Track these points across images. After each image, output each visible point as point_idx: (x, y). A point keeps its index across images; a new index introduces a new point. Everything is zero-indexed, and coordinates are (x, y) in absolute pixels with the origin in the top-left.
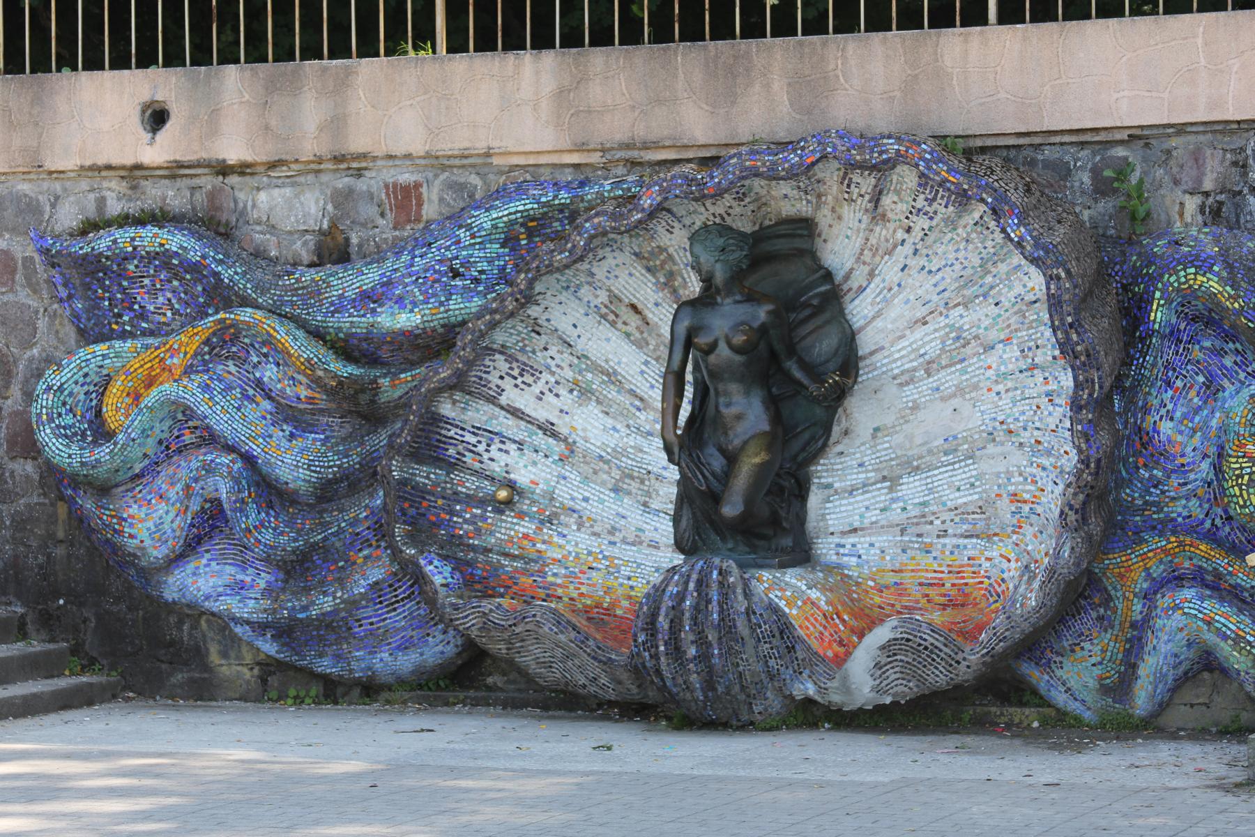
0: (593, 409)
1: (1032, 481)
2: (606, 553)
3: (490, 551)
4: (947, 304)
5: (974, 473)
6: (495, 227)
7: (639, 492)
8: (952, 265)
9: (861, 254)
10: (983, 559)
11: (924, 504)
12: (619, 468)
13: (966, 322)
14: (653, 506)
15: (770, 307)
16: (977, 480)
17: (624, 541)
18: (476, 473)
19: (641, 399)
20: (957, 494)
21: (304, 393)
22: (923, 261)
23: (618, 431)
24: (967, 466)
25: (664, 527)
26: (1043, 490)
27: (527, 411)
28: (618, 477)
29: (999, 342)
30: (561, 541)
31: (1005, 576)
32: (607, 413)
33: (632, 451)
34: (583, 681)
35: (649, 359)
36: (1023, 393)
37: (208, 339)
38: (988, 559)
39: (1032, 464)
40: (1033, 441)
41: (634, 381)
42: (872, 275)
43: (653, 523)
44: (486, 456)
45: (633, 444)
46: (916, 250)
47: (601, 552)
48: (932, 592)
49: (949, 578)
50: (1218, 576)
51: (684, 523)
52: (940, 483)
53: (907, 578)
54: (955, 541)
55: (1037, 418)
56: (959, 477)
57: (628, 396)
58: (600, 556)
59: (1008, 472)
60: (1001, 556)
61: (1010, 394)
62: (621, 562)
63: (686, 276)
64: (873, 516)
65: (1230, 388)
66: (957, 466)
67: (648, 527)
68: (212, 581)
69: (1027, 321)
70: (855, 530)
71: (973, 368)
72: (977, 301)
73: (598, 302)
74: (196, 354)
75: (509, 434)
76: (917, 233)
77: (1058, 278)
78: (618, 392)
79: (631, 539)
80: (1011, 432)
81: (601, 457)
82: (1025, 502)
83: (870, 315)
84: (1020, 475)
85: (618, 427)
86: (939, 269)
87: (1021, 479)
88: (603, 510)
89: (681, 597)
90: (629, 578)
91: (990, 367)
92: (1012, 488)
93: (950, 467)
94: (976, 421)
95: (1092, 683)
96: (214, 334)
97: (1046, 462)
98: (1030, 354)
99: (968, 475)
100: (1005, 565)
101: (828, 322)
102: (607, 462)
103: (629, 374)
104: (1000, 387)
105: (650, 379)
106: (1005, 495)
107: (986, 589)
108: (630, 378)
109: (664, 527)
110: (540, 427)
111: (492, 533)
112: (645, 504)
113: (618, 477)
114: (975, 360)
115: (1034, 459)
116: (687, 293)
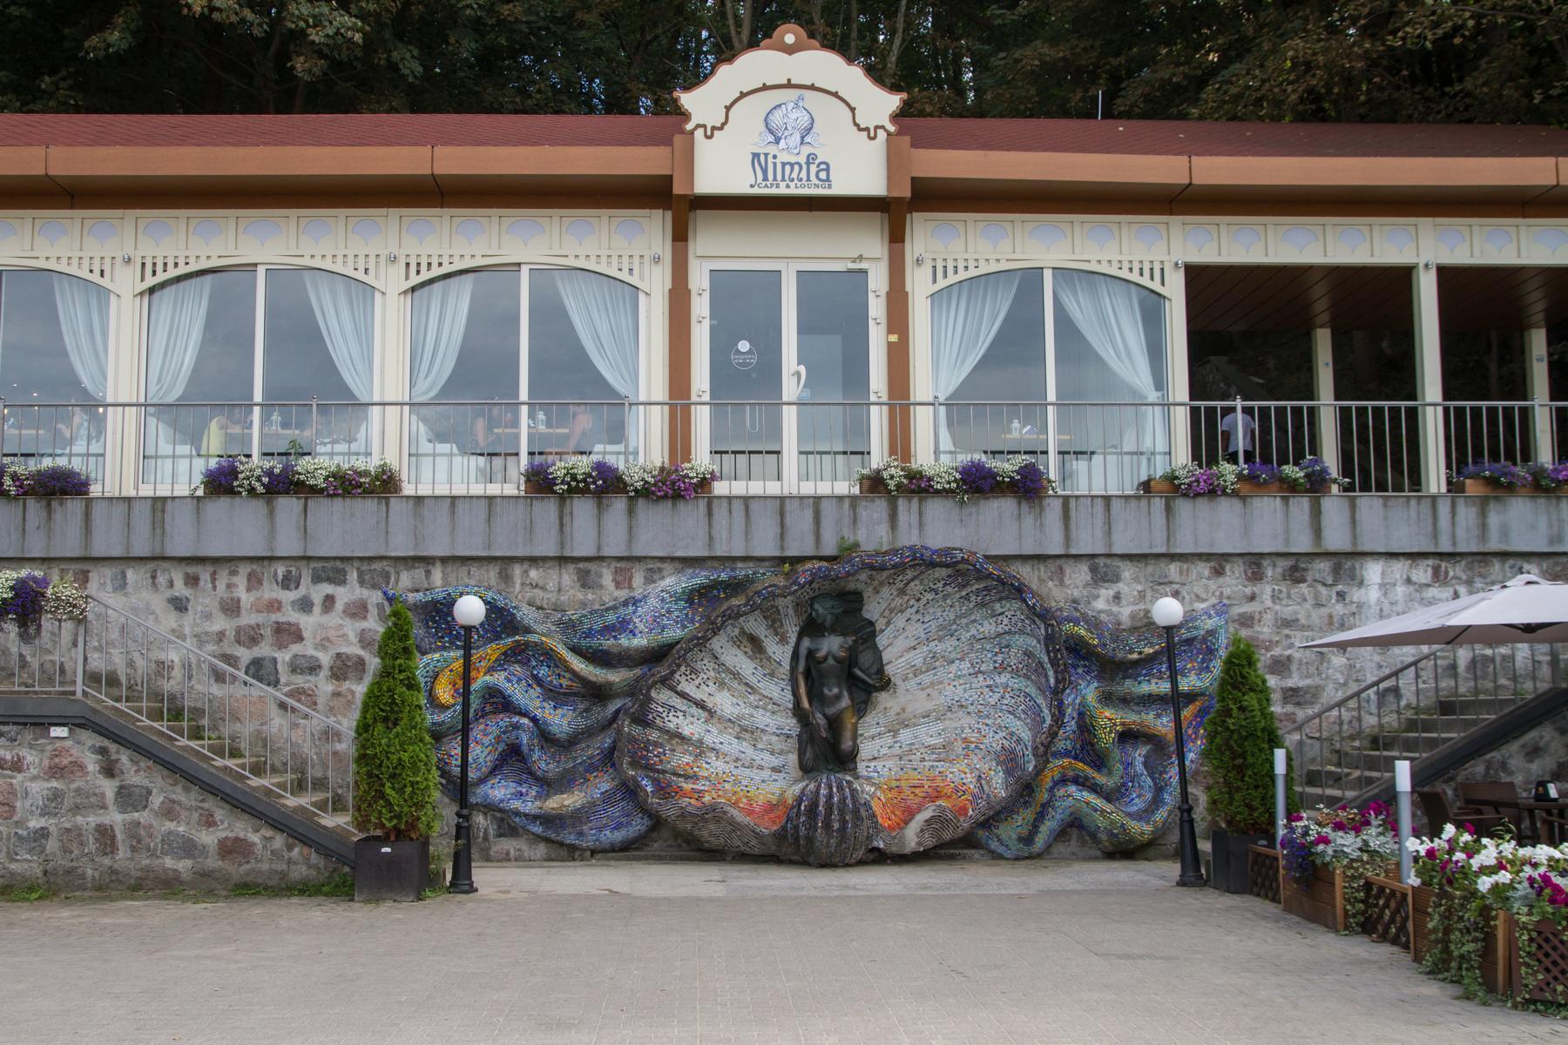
0: (725, 693)
3: (666, 772)
6: (684, 592)
11: (912, 744)
12: (739, 725)
13: (938, 650)
15: (854, 638)
17: (743, 766)
18: (660, 729)
19: (752, 688)
21: (565, 682)
22: (919, 616)
27: (691, 694)
30: (708, 766)
31: (965, 781)
34: (739, 843)
37: (506, 652)
38: (951, 773)
42: (888, 624)
44: (666, 719)
48: (917, 791)
50: (1086, 778)
51: (808, 755)
53: (903, 784)
54: (931, 763)
59: (962, 727)
61: (963, 686)
64: (884, 751)
65: (1084, 684)
68: (503, 792)
70: (875, 758)
73: (733, 635)
74: (496, 660)
75: (678, 707)
76: (924, 601)
77: (1053, 625)
80: (962, 706)
82: (972, 742)
83: (886, 644)
89: (830, 796)
92: (964, 736)
94: (942, 700)
95: (1014, 836)
96: (510, 649)
97: (989, 722)
100: (963, 776)
101: (867, 648)
102: (733, 723)
104: (956, 683)
110: (695, 703)
111: (669, 762)
112: (754, 745)
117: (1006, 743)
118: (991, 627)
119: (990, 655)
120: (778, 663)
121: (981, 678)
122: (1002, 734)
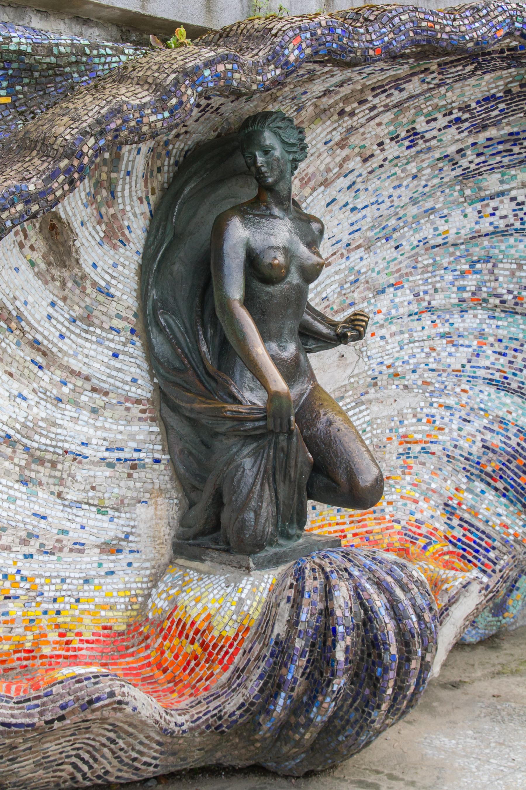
1: (428, 421)
2: (24, 573)
4: (348, 245)
5: (367, 418)
7: (51, 481)
8: (383, 202)
12: (27, 449)
13: (362, 266)
14: (69, 497)
16: (368, 425)
23: (24, 399)
24: (361, 412)
25: (91, 523)
26: (440, 429)
28: (23, 463)
29: (389, 286)
31: (418, 516)
32: (11, 375)
33: (43, 425)
35: (55, 299)
36: (411, 336)
39: (431, 405)
40: (420, 382)
41: (40, 329)
43: (78, 519)
45: (43, 415)
46: (354, 183)
47: (19, 571)
49: (352, 528)
55: (431, 360)
57: (28, 349)
58: (18, 578)
60: (402, 497)
61: (398, 338)
62: (43, 580)
63: (119, 188)
67: (73, 526)
69: (419, 265)
72: (379, 244)
78: (18, 344)
79: (47, 548)
80: (396, 375)
81: (9, 436)
82: (416, 442)
85: (25, 393)
88: (17, 513)
90: (55, 600)
91: (379, 312)
92: (402, 431)
97: (451, 401)
98: (427, 298)
99: (362, 421)
103: (35, 319)
104: (383, 332)
105: (59, 326)
107: (399, 533)
108: (36, 325)
109: (91, 523)
112: (59, 495)
113: (23, 463)
115: (434, 400)
116: (112, 211)
117: (495, 440)
118: (465, 221)
119: (449, 277)
120: (100, 290)
122: (478, 423)
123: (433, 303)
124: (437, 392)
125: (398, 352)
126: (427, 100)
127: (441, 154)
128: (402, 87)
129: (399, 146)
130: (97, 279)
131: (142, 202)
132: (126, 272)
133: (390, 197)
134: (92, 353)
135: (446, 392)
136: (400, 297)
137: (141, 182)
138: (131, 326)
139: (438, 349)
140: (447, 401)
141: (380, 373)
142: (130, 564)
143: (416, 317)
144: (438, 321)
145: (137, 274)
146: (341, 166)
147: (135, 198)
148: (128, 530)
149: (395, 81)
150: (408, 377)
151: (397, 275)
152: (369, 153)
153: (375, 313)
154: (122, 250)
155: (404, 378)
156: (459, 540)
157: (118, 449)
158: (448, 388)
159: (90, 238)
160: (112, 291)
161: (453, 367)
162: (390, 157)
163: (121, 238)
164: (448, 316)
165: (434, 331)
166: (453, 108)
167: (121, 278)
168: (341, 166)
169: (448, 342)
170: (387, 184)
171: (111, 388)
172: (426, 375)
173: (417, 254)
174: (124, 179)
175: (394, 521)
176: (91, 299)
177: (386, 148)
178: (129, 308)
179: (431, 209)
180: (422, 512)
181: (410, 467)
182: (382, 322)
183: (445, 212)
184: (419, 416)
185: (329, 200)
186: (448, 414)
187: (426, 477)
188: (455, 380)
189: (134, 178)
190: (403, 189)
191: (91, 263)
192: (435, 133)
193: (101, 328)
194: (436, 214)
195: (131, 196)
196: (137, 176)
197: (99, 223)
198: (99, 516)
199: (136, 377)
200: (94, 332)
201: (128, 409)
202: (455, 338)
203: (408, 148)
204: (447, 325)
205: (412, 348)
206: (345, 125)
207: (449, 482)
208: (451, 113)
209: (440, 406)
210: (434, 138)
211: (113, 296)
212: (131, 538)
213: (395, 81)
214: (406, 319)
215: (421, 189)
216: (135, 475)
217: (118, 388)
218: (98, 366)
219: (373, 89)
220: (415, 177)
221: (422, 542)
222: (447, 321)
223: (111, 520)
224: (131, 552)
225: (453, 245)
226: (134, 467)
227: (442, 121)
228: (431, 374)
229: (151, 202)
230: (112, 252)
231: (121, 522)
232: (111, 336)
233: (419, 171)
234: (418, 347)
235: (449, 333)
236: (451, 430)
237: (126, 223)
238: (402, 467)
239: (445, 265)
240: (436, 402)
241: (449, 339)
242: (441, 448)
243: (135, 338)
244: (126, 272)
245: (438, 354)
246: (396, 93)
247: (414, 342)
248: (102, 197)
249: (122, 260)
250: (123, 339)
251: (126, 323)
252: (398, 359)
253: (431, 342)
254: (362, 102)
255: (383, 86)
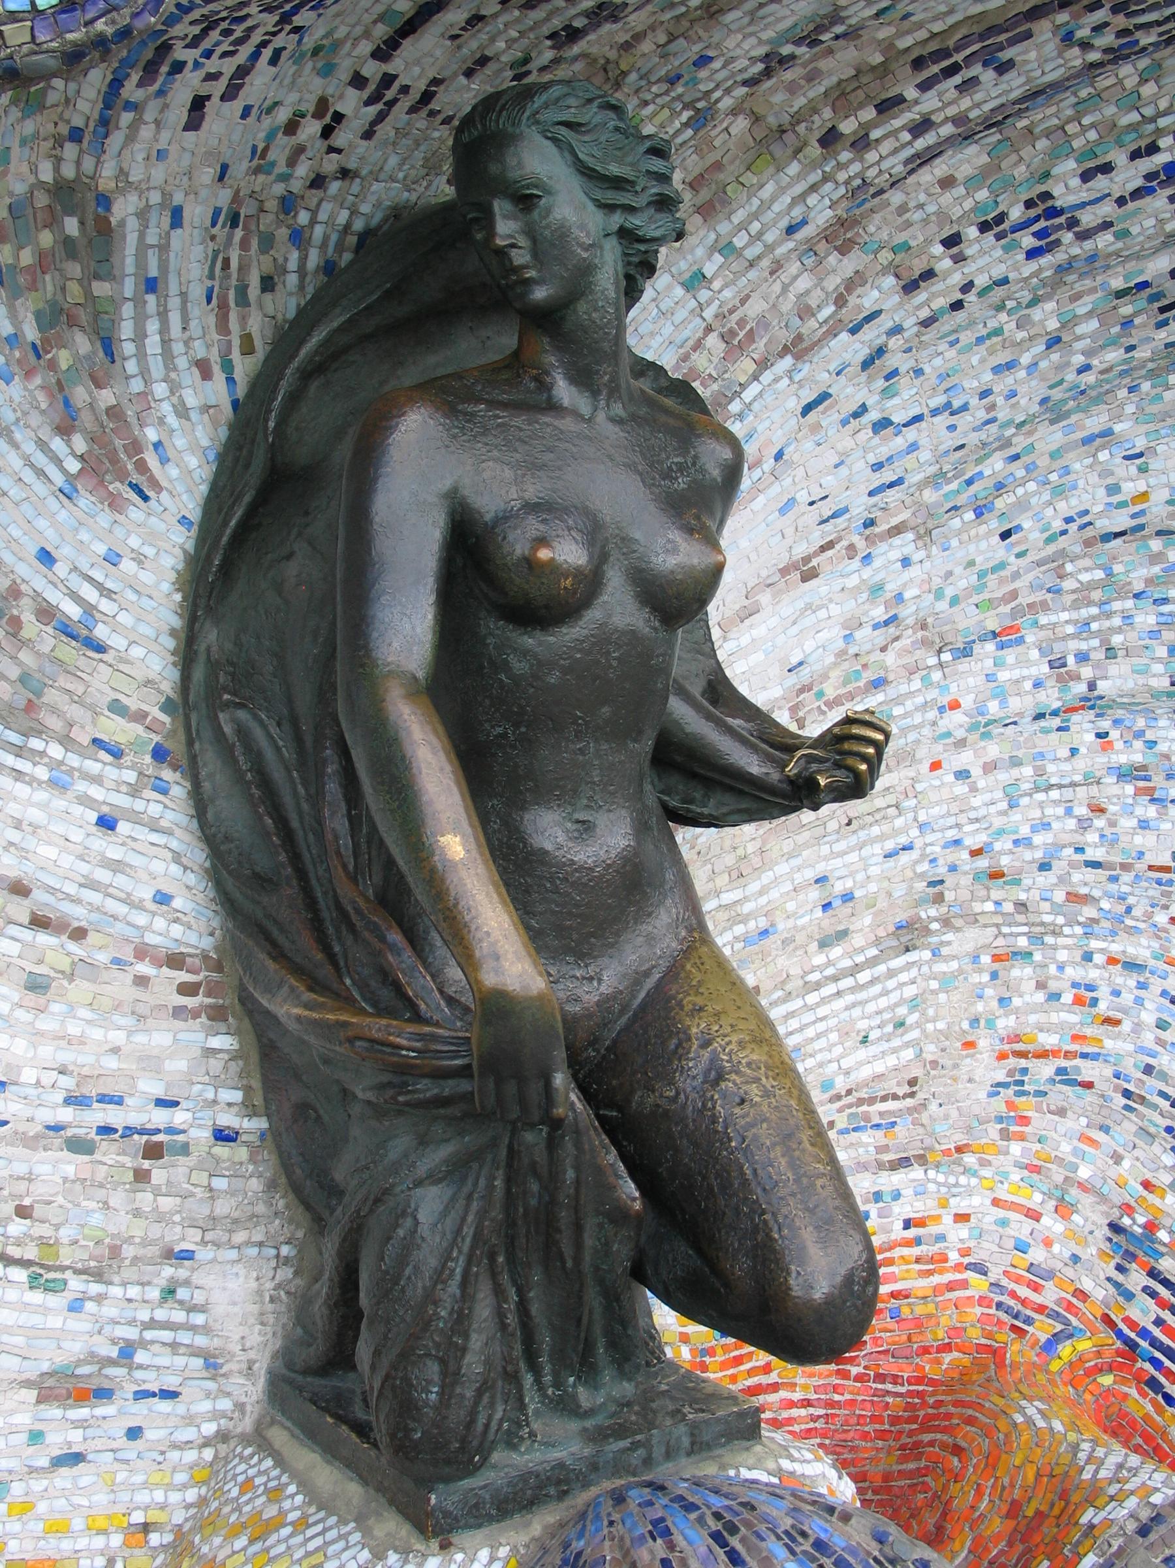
1: (1078, 1001)
4: (870, 523)
5: (910, 991)
8: (965, 408)
9: (698, 345)
10: (948, 1219)
20: (862, 1053)
24: (891, 974)
26: (1108, 1021)
29: (983, 639)
31: (1037, 1255)
36: (1040, 772)
38: (962, 1218)
39: (1088, 957)
40: (1059, 896)
46: (881, 351)
52: (821, 1027)
56: (871, 1007)
60: (996, 1202)
61: (1003, 776)
63: (126, 330)
66: (864, 977)
69: (1068, 584)
71: (909, 705)
72: (956, 523)
82: (1043, 1054)
84: (1041, 985)
86: (918, 419)
87: (1040, 997)
91: (955, 705)
92: (1006, 1023)
93: (848, 982)
97: (1141, 949)
98: (1087, 672)
99: (894, 997)
100: (1021, 1227)
104: (965, 759)
106: (982, 1043)
107: (982, 1301)
114: (916, 684)
115: (1095, 944)
116: (106, 397)
120: (67, 631)
121: (1083, 728)
123: (1103, 687)
124: (1105, 924)
125: (1004, 813)
126: (1081, 109)
127: (1126, 278)
128: (1005, 55)
129: (1007, 249)
130: (54, 596)
131: (206, 375)
132: (146, 577)
133: (985, 394)
134: (35, 815)
135: (1129, 922)
136: (1012, 668)
137: (202, 316)
138: (156, 738)
139: (1112, 809)
140: (1131, 950)
141: (953, 868)
142: (134, 1433)
143: (1056, 722)
144: (1114, 734)
145: (181, 584)
146: (840, 302)
147: (182, 362)
148: (132, 1333)
149: (982, 37)
150: (1027, 882)
151: (1006, 609)
152: (919, 266)
153: (941, 709)
154: (136, 513)
155: (1017, 882)
156: (1144, 1333)
157: (103, 1099)
158: (1136, 912)
159: (28, 476)
160: (101, 632)
161: (1151, 859)
162: (981, 281)
163: (136, 478)
164: (1141, 723)
165: (1102, 759)
166: (1160, 132)
167: (132, 597)
168: (840, 302)
169: (1138, 792)
170: (975, 360)
171: (94, 917)
172: (1076, 877)
173: (1062, 553)
174: (139, 303)
175: (968, 1267)
176: (38, 654)
177: (969, 252)
178: (148, 683)
179: (1102, 435)
180: (1048, 1243)
181: (1024, 1120)
182: (960, 734)
183: (1140, 444)
184: (1053, 986)
185: (808, 396)
186: (1132, 983)
187: (1065, 1148)
188: (1155, 892)
189: (174, 303)
190: (1022, 374)
191: (33, 549)
192: (1107, 209)
193: (66, 741)
194: (1114, 450)
195: (167, 355)
196: (184, 295)
197: (64, 430)
198: (37, 1297)
199: (167, 889)
200: (43, 754)
201: (141, 981)
202: (1158, 780)
203: (1032, 254)
204: (1138, 744)
205: (1041, 805)
206: (842, 176)
207: (1126, 1164)
208: (1153, 149)
209: (1112, 961)
210: (1106, 225)
211: (101, 648)
212: (140, 1357)
213: (982, 37)
214: (1028, 727)
215: (1070, 377)
216: (158, 1176)
217: (115, 917)
218: (48, 852)
219: (918, 64)
220: (1054, 342)
221: (1041, 1329)
222: (1139, 734)
223: (75, 1307)
224: (142, 1395)
225: (1159, 533)
226: (154, 1152)
227: (1129, 176)
228: (1090, 874)
229: (239, 374)
230: (104, 518)
231: (109, 1311)
232: (93, 767)
233: (1063, 326)
234: (1056, 803)
235: (1144, 768)
236: (1138, 1027)
237: (152, 434)
238: (1000, 1120)
239: (1138, 586)
240: (1102, 951)
241: (1141, 784)
242: (1108, 1072)
243: (167, 774)
244: (146, 577)
245: (1112, 824)
246: (988, 76)
247: (1051, 787)
248: (76, 356)
249: (134, 542)
250: (131, 776)
251: (139, 729)
252: (1001, 832)
253: (1094, 791)
254: (887, 107)
255: (944, 53)
